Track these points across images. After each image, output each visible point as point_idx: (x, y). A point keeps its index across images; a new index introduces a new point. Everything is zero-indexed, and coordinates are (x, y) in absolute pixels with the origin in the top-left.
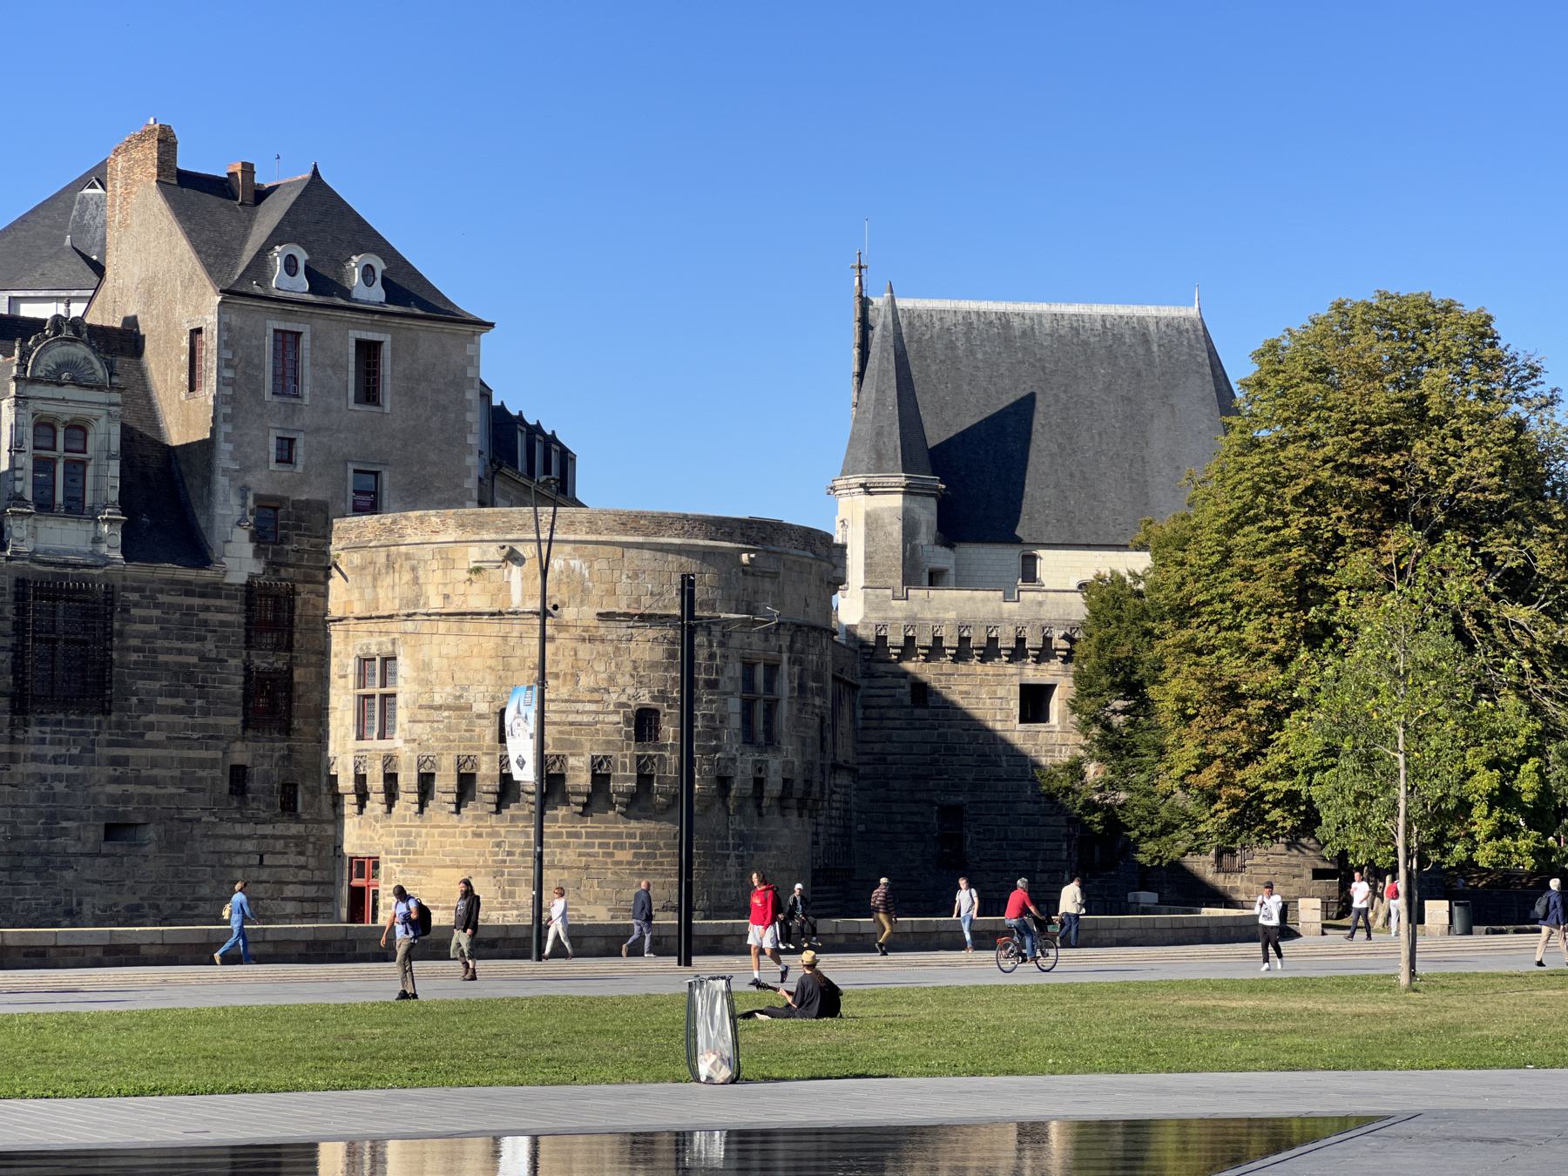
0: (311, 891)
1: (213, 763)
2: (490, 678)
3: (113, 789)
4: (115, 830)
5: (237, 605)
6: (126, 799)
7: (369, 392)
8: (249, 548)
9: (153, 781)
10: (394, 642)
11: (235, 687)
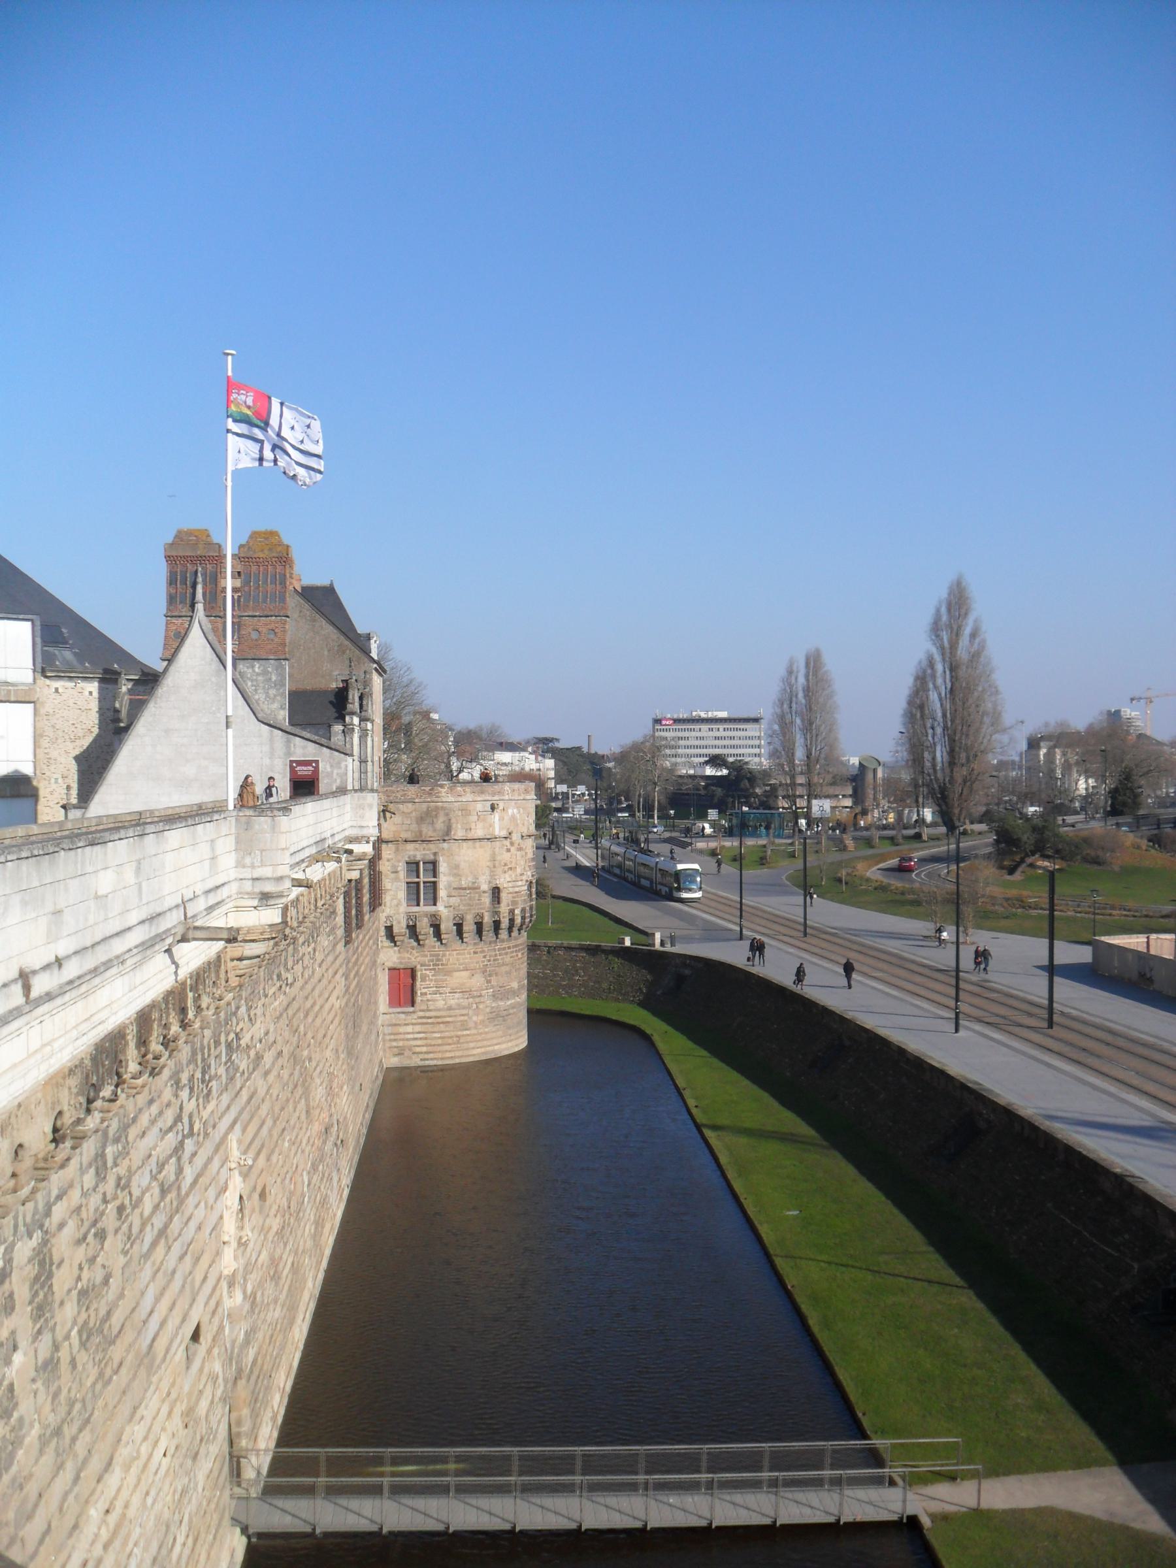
2: (487, 872)
10: (435, 854)
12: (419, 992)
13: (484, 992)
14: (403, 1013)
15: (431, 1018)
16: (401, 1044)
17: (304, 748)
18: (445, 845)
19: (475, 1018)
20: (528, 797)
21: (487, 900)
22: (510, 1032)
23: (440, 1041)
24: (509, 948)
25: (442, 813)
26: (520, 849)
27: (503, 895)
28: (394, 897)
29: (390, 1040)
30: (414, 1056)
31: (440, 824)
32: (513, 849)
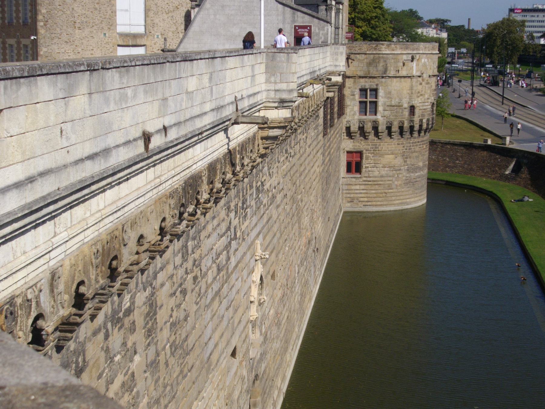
2: (408, 97)
10: (377, 85)
12: (364, 166)
13: (402, 168)
14: (354, 178)
15: (370, 181)
16: (352, 196)
17: (303, 18)
18: (383, 80)
19: (396, 183)
20: (434, 52)
21: (406, 113)
22: (417, 191)
23: (375, 195)
24: (418, 142)
25: (382, 60)
26: (428, 83)
27: (417, 111)
28: (353, 109)
29: (346, 193)
30: (360, 203)
31: (380, 67)
32: (423, 83)
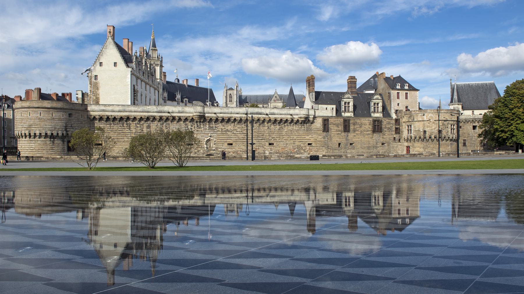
0: (402, 150)
1: (392, 137)
2: (422, 127)
3: (382, 140)
4: (383, 144)
5: (394, 121)
6: (384, 141)
7: (406, 98)
8: (395, 115)
9: (386, 139)
11: (394, 129)
21: (422, 133)
27: (427, 133)
28: (405, 133)
31: (412, 118)
